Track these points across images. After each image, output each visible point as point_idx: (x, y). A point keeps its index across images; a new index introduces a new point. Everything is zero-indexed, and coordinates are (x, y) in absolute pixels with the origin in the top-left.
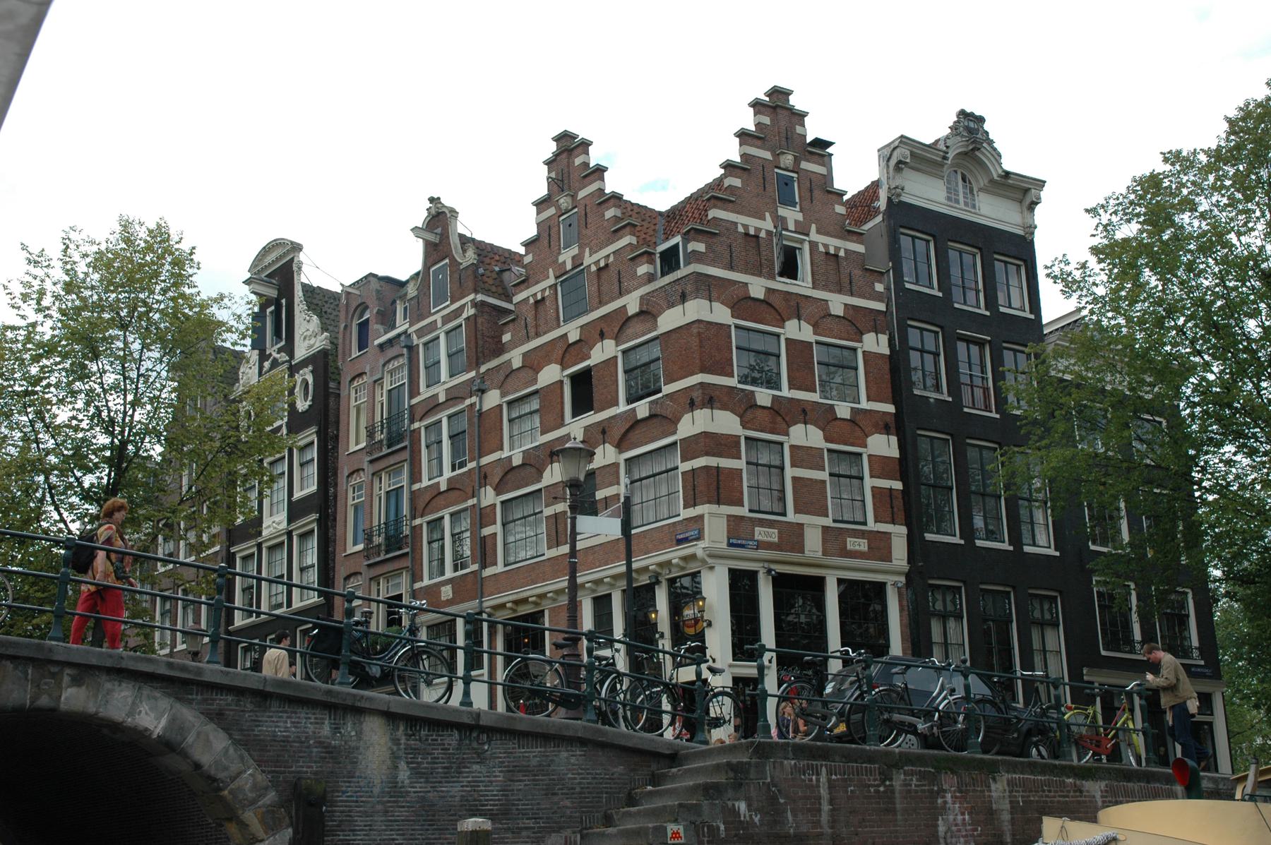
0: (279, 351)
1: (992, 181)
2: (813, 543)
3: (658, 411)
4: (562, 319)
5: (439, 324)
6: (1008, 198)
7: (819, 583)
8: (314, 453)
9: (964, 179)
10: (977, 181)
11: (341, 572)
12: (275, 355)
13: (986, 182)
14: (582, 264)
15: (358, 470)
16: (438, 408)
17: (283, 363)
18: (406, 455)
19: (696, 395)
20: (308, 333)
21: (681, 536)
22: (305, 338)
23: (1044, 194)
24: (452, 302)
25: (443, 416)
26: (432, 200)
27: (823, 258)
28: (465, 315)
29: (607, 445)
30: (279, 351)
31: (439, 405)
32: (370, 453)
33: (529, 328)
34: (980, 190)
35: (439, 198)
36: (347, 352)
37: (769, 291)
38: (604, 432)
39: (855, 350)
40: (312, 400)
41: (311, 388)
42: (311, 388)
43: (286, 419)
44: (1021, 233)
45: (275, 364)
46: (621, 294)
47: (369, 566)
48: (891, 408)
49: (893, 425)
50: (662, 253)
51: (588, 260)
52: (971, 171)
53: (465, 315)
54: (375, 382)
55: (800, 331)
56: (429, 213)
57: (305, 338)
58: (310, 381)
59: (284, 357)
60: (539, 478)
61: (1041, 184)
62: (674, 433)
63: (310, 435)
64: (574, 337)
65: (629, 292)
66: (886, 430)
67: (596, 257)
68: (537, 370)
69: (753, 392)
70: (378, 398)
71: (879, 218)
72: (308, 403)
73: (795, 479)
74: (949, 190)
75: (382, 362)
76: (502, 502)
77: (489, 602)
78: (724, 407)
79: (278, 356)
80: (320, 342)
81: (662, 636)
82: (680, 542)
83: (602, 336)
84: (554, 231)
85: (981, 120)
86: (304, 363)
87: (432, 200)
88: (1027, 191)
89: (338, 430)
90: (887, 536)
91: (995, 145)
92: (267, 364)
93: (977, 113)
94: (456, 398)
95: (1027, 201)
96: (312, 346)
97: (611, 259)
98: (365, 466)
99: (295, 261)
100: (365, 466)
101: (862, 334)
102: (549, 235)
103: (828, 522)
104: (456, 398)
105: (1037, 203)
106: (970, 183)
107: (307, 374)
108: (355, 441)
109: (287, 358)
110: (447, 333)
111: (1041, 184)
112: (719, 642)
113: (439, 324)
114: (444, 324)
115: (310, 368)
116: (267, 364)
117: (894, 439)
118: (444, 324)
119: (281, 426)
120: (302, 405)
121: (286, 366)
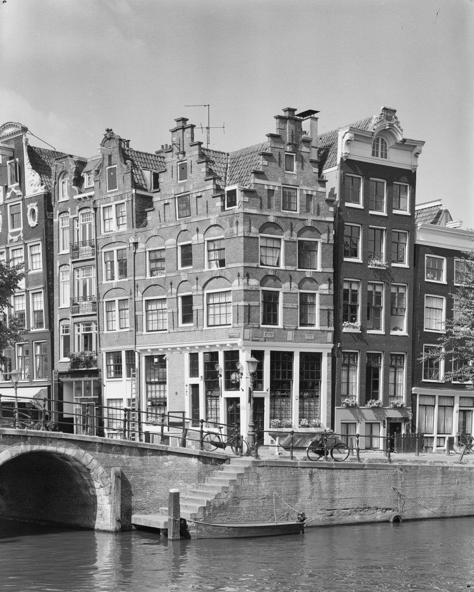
0: (16, 188)
1: (397, 143)
3: (223, 275)
4: (177, 216)
5: (112, 199)
6: (405, 150)
7: (291, 354)
8: (39, 250)
9: (382, 143)
10: (389, 143)
11: (57, 317)
12: (13, 190)
13: (394, 143)
15: (65, 265)
17: (19, 196)
18: (94, 262)
19: (242, 271)
20: (34, 183)
21: (231, 335)
22: (32, 185)
23: (424, 148)
25: (115, 249)
26: (108, 130)
27: (305, 198)
30: (16, 188)
32: (73, 258)
33: (161, 217)
34: (391, 147)
35: (111, 130)
36: (56, 198)
40: (38, 222)
41: (37, 214)
42: (37, 214)
43: (21, 229)
44: (410, 169)
45: (14, 195)
47: (73, 317)
49: (332, 279)
50: (228, 192)
52: (386, 137)
54: (74, 218)
57: (32, 185)
58: (36, 211)
59: (19, 192)
61: (423, 143)
63: (38, 241)
70: (76, 227)
71: (336, 168)
72: (35, 223)
74: (373, 148)
75: (78, 208)
76: (146, 300)
77: (138, 348)
79: (16, 191)
80: (41, 190)
81: (221, 376)
82: (230, 337)
84: (175, 170)
85: (395, 111)
86: (31, 200)
87: (108, 130)
88: (415, 146)
89: (53, 239)
91: (400, 125)
92: (9, 195)
95: (415, 152)
96: (36, 191)
98: (70, 263)
99: (24, 138)
100: (70, 263)
102: (172, 171)
105: (418, 154)
106: (385, 144)
107: (33, 206)
108: (63, 249)
109: (21, 194)
110: (116, 205)
111: (423, 143)
112: (245, 382)
115: (36, 204)
116: (9, 195)
119: (18, 232)
120: (32, 223)
121: (20, 198)
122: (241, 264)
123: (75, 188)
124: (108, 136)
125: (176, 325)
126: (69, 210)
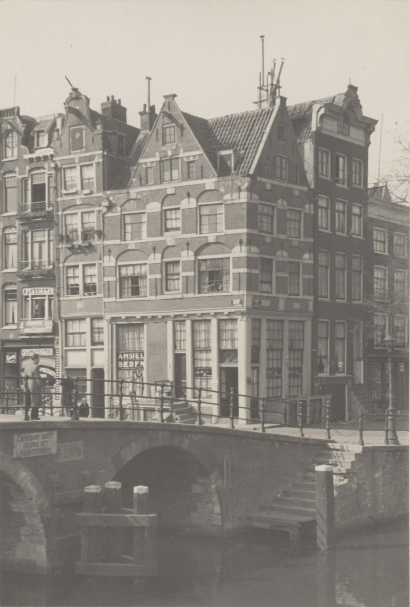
2: (282, 305)
5: (77, 161)
14: (178, 155)
16: (76, 207)
19: (244, 238)
24: (87, 151)
25: (79, 212)
28: (96, 160)
29: (190, 251)
31: (76, 205)
37: (273, 186)
38: (188, 244)
39: (300, 212)
46: (202, 177)
48: (311, 240)
51: (181, 154)
53: (96, 160)
55: (281, 203)
56: (71, 96)
60: (146, 258)
61: (376, 122)
62: (230, 252)
64: (170, 191)
65: (207, 177)
66: (310, 251)
67: (187, 154)
68: (148, 202)
69: (264, 236)
73: (277, 277)
75: (28, 168)
78: (253, 245)
83: (189, 195)
90: (307, 300)
93: (355, 86)
94: (90, 205)
97: (197, 158)
98: (17, 225)
101: (304, 204)
103: (286, 296)
104: (90, 205)
111: (376, 122)
113: (77, 161)
114: (80, 161)
117: (312, 255)
118: (80, 161)
122: (245, 231)
123: (25, 148)
124: (74, 95)
125: (159, 290)
126: (17, 170)
